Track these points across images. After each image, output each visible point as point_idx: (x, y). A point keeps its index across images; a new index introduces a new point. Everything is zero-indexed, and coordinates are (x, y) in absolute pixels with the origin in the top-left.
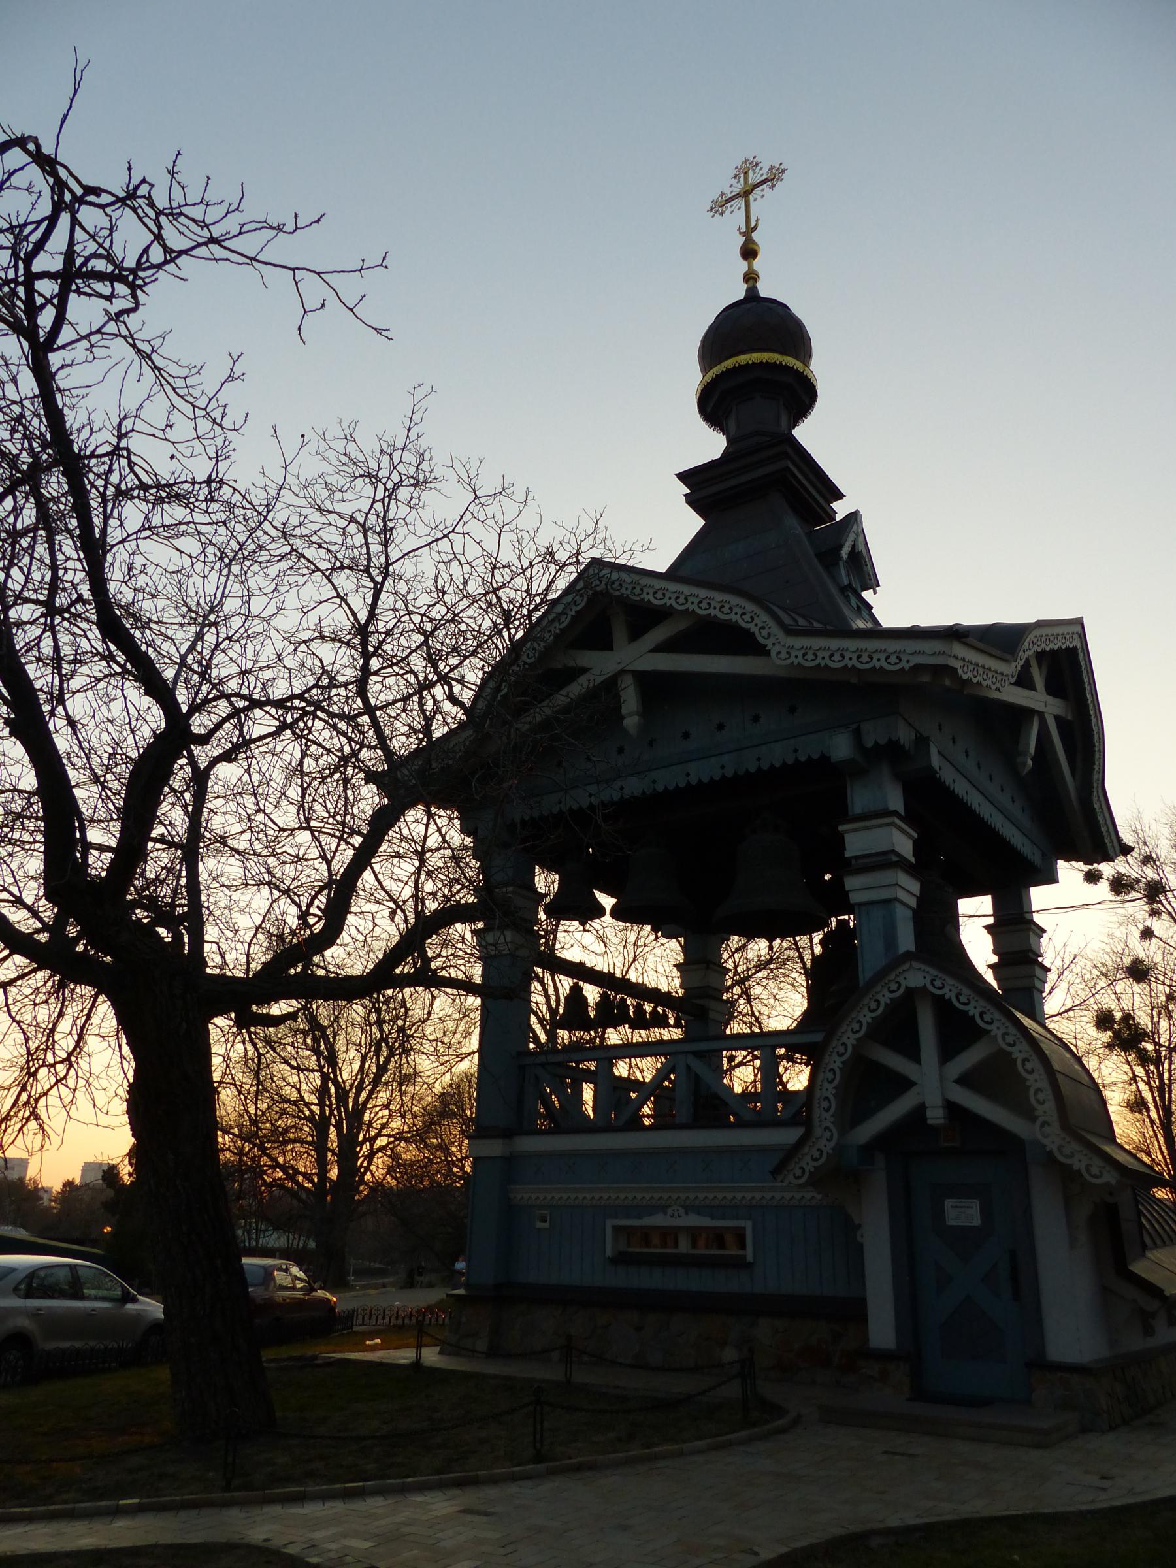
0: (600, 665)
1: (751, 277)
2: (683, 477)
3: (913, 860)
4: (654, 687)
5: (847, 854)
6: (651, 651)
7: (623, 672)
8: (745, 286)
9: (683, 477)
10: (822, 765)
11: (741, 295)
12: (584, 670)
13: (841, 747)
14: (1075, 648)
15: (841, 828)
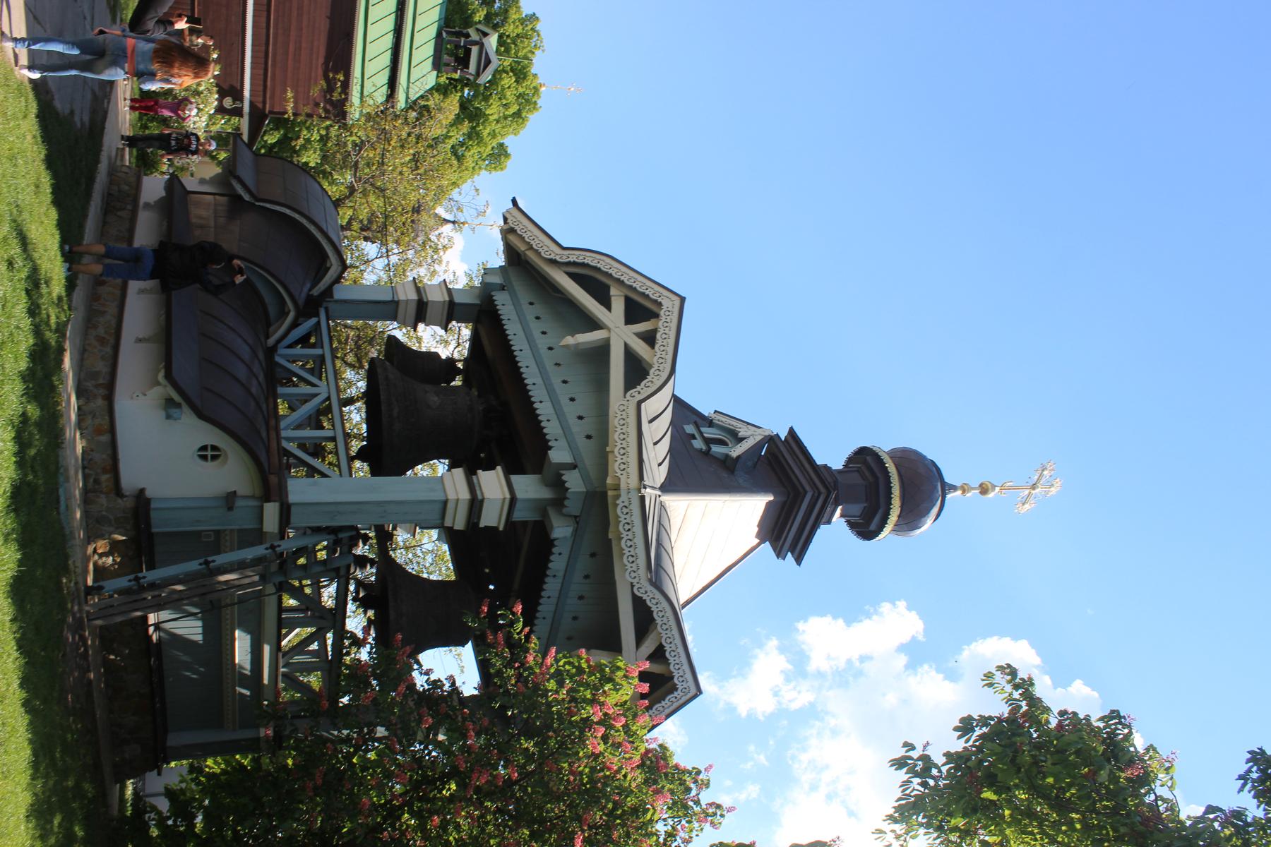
0: (613, 317)
1: (965, 489)
2: (792, 432)
3: (482, 525)
4: (601, 353)
5: (480, 472)
6: (626, 345)
7: (609, 330)
8: (958, 485)
9: (792, 432)
10: (543, 445)
11: (948, 479)
12: (609, 308)
13: (559, 455)
14: (674, 688)
15: (499, 468)
